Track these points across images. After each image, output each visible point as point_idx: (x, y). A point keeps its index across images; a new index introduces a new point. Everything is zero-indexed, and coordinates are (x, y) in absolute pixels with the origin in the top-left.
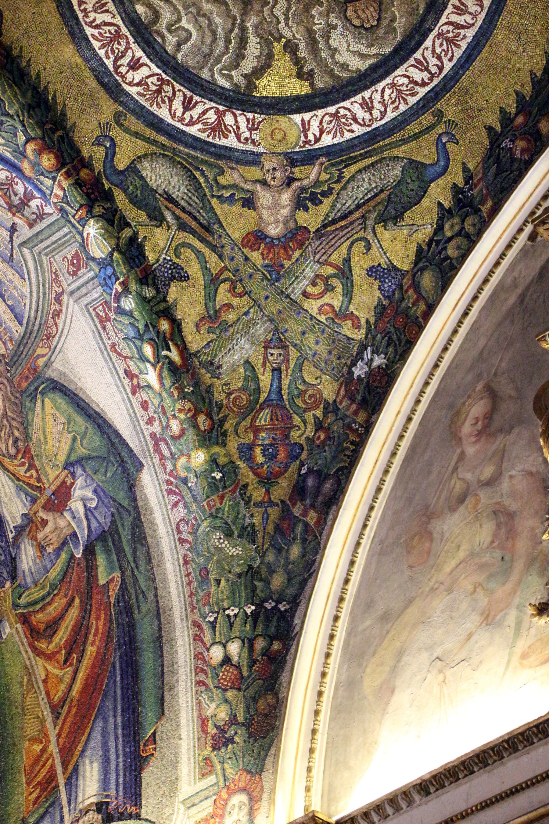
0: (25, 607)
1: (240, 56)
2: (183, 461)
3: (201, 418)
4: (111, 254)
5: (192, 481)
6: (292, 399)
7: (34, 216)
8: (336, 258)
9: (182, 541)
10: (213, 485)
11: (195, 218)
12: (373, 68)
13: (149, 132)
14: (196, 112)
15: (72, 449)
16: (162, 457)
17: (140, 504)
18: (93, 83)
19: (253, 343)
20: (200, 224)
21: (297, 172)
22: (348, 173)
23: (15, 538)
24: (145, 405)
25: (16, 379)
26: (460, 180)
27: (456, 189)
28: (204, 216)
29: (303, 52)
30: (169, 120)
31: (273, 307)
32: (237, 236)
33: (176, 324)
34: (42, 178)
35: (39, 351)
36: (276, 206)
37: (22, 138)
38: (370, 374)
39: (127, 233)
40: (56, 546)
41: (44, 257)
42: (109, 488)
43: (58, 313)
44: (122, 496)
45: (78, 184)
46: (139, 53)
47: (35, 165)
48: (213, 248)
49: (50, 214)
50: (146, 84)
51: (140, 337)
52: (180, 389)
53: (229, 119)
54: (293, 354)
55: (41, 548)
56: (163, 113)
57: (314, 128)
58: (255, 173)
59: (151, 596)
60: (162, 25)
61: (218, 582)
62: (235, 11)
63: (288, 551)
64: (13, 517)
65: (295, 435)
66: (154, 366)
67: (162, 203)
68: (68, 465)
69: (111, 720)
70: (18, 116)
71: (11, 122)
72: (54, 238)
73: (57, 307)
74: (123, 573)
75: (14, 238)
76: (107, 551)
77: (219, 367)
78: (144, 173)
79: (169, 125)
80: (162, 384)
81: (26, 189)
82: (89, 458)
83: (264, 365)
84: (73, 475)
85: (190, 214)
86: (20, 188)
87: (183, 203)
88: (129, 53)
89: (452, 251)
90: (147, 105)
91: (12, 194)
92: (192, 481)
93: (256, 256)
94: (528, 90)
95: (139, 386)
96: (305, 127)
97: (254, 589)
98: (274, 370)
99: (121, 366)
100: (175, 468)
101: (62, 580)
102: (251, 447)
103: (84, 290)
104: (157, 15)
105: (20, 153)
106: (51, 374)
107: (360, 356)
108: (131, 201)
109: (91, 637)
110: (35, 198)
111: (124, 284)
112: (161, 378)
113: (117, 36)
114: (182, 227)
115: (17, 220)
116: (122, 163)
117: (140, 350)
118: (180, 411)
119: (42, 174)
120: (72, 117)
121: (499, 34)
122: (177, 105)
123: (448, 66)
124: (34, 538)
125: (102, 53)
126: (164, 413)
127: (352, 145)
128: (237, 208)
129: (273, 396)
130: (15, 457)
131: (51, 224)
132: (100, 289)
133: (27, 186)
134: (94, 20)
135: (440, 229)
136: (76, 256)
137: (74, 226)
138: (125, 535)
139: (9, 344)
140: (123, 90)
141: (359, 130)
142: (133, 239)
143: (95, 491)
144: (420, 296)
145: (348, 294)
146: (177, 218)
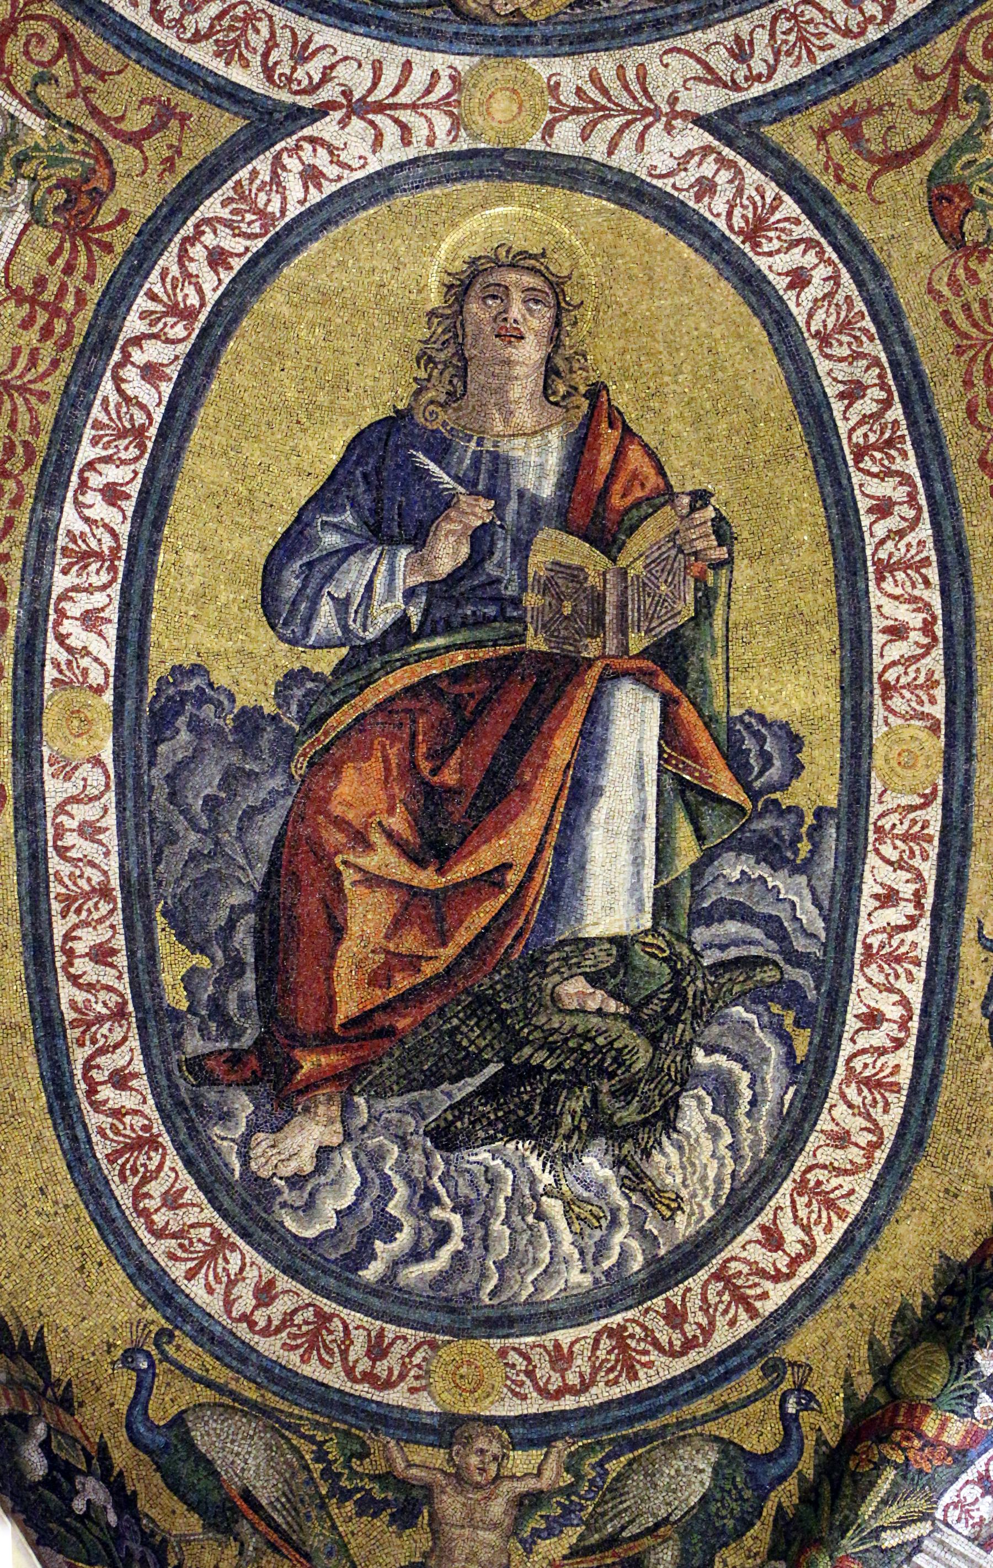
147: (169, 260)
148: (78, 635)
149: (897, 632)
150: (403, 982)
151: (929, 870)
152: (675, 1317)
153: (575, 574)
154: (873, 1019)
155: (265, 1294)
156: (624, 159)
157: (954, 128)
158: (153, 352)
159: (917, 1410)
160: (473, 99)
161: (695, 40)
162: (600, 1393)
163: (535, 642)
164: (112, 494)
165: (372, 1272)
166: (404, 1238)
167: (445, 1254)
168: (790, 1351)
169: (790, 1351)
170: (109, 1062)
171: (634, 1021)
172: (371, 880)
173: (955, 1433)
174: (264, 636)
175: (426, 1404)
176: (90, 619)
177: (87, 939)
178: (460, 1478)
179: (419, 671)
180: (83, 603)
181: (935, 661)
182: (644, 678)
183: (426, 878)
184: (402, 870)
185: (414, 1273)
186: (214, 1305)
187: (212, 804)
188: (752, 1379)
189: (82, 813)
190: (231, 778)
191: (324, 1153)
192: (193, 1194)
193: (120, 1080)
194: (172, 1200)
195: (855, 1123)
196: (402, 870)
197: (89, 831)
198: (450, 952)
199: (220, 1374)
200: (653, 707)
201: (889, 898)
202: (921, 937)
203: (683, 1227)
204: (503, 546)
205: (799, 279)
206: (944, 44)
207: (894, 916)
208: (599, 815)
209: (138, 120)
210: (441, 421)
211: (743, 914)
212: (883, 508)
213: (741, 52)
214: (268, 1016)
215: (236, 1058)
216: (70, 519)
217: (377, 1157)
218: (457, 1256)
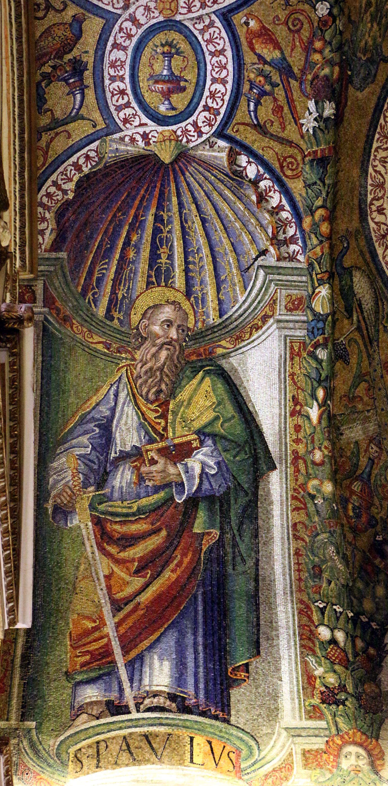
0: (103, 513)
4: (328, 315)
5: (319, 501)
7: (287, 255)
9: (296, 538)
11: (367, 329)
13: (368, 256)
15: (211, 423)
16: (297, 471)
17: (260, 492)
18: (356, 202)
19: (364, 433)
20: (369, 335)
23: (117, 459)
24: (298, 428)
25: (190, 350)
30: (381, 258)
34: (313, 236)
35: (223, 343)
37: (319, 202)
40: (158, 483)
41: (273, 285)
42: (234, 468)
43: (258, 328)
47: (315, 226)
48: (369, 356)
49: (299, 261)
50: (380, 226)
51: (319, 382)
55: (141, 479)
59: (250, 563)
61: (329, 582)
63: (374, 588)
65: (374, 510)
66: (320, 406)
67: (355, 305)
68: (199, 432)
69: (190, 638)
70: (328, 187)
71: (321, 188)
72: (290, 278)
73: (260, 323)
74: (223, 533)
75: (259, 259)
76: (210, 510)
77: (342, 434)
78: (355, 279)
79: (379, 261)
80: (320, 422)
81: (295, 234)
82: (223, 437)
83: (366, 451)
84: (202, 443)
85: (366, 324)
86: (291, 231)
87: (365, 314)
88: (382, 201)
90: (375, 239)
91: (281, 231)
92: (319, 501)
95: (299, 412)
97: (352, 602)
98: (370, 459)
100: (306, 483)
101: (154, 511)
103: (291, 325)
105: (311, 210)
106: (224, 363)
108: (340, 290)
109: (172, 566)
110: (297, 244)
112: (320, 418)
115: (271, 249)
118: (326, 447)
119: (315, 234)
124: (137, 469)
125: (370, 188)
126: (313, 442)
129: (365, 476)
130: (152, 403)
131: (296, 268)
132: (304, 332)
133: (298, 233)
134: (376, 166)
136: (300, 300)
137: (312, 280)
139: (200, 325)
140: (367, 220)
143: (218, 464)
146: (359, 321)
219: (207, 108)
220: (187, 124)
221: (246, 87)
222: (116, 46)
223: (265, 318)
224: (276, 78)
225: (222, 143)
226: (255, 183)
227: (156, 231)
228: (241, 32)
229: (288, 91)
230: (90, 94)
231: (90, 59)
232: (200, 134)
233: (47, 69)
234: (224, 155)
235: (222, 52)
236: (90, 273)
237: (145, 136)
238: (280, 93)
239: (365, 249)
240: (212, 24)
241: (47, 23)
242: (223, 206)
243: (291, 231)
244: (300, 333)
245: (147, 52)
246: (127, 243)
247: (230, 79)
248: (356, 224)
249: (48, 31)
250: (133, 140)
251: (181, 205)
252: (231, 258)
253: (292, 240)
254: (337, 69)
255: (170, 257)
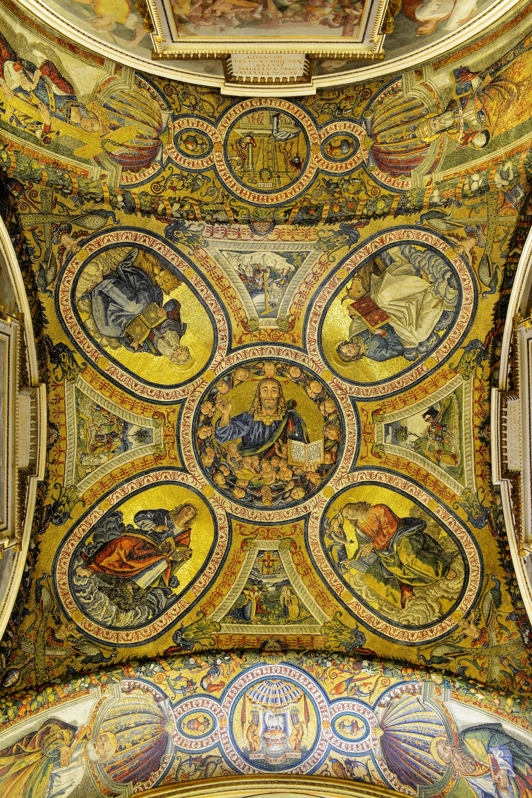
1: (434, 610)
2: (507, 707)
3: (501, 693)
6: (520, 667)
8: (496, 625)
10: (519, 704)
12: (464, 582)
13: (428, 646)
14: (435, 631)
18: (407, 648)
21: (469, 619)
22: (480, 607)
24: (486, 707)
26: (505, 581)
27: (506, 583)
28: (458, 650)
29: (446, 595)
31: (494, 652)
32: (469, 646)
33: (475, 680)
36: (472, 631)
38: (529, 637)
39: (443, 671)
44: (506, 741)
45: (421, 670)
46: (411, 632)
47: (408, 676)
52: (489, 691)
53: (443, 625)
54: (509, 657)
56: (428, 638)
57: (464, 607)
58: (460, 629)
60: (411, 621)
62: (424, 602)
64: (492, 789)
67: (445, 657)
86: (410, 687)
89: (517, 593)
92: (514, 709)
93: (479, 646)
94: (499, 550)
96: (462, 609)
99: (471, 704)
102: (521, 688)
104: (408, 621)
106: (461, 730)
107: (523, 638)
111: (453, 681)
113: (404, 633)
114: (455, 657)
116: (428, 658)
117: (471, 693)
120: (408, 659)
121: (482, 548)
122: (430, 633)
123: (479, 565)
127: (475, 601)
128: (463, 640)
135: (511, 593)
138: (517, 750)
141: (474, 597)
142: (446, 671)
144: (521, 609)
145: (507, 630)
147: (161, 472)
148: (114, 497)
149: (200, 583)
150: (111, 568)
151: (182, 611)
152: (108, 633)
153: (170, 545)
154: (161, 621)
155: (64, 584)
156: (215, 509)
157: (251, 536)
158: (150, 479)
159: (130, 666)
160: (206, 488)
161: (233, 504)
162: (91, 633)
163: (160, 547)
164: (132, 488)
165: (78, 594)
166: (85, 595)
167: (87, 601)
168: (118, 649)
169: (118, 649)
170: (73, 542)
171: (133, 597)
172: (118, 554)
173: (132, 673)
174: (132, 517)
175: (70, 614)
176: (117, 497)
177: (84, 527)
178: (67, 626)
179: (145, 538)
180: (118, 495)
181: (202, 589)
182: (168, 562)
183: (125, 560)
184: (123, 556)
185: (82, 600)
186: (58, 579)
187: (110, 529)
188: (111, 648)
189: (97, 514)
190: (114, 528)
191: (85, 576)
192: (68, 565)
193: (72, 545)
194: (65, 563)
195: (149, 631)
196: (123, 556)
197: (95, 517)
198: (120, 570)
199: (51, 587)
200: (166, 566)
201: (175, 610)
202: (175, 617)
203: (118, 625)
204: (166, 535)
205: (222, 537)
206: (258, 527)
207: (174, 613)
208: (150, 572)
209: (172, 456)
210: (171, 516)
211: (156, 597)
212: (210, 569)
213: (236, 509)
214: (94, 555)
215: (86, 556)
216: (126, 485)
217: (91, 583)
218: (88, 603)
219: (363, 713)
220: (369, 722)
221: (356, 697)
222: (340, 746)
223: (443, 706)
224: (353, 684)
225: (377, 708)
226: (392, 698)
227: (409, 743)
228: (336, 697)
229: (358, 680)
230: (358, 759)
231: (345, 757)
232: (372, 717)
233: (349, 774)
234: (381, 709)
235: (343, 705)
236: (424, 776)
237: (374, 740)
238: (358, 683)
239: (426, 646)
240: (333, 708)
241: (332, 772)
242: (400, 713)
243: (410, 687)
244: (449, 692)
245: (342, 734)
246: (414, 757)
247: (353, 703)
248: (415, 649)
249: (335, 772)
250: (375, 745)
251: (399, 731)
252: (419, 714)
253: (414, 686)
254: (351, 659)
255: (419, 740)
